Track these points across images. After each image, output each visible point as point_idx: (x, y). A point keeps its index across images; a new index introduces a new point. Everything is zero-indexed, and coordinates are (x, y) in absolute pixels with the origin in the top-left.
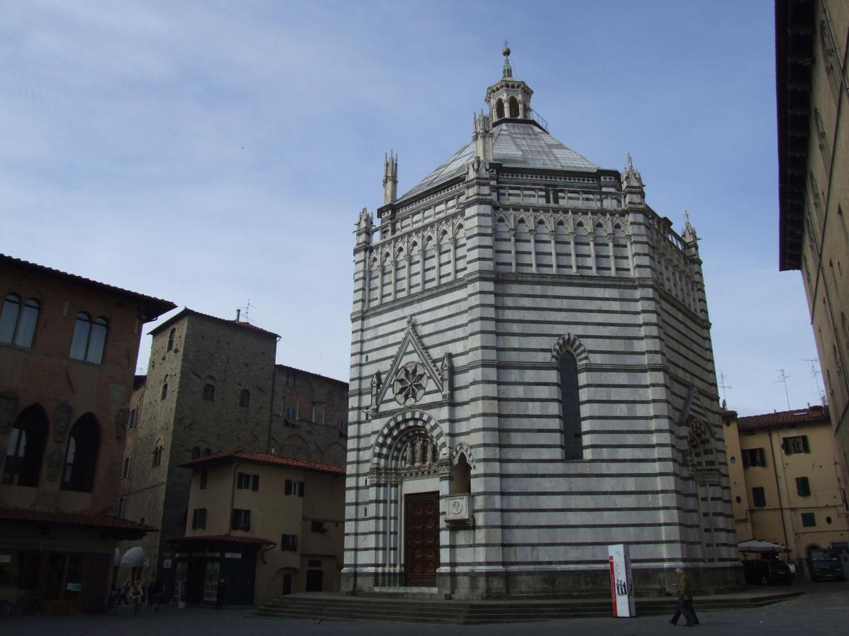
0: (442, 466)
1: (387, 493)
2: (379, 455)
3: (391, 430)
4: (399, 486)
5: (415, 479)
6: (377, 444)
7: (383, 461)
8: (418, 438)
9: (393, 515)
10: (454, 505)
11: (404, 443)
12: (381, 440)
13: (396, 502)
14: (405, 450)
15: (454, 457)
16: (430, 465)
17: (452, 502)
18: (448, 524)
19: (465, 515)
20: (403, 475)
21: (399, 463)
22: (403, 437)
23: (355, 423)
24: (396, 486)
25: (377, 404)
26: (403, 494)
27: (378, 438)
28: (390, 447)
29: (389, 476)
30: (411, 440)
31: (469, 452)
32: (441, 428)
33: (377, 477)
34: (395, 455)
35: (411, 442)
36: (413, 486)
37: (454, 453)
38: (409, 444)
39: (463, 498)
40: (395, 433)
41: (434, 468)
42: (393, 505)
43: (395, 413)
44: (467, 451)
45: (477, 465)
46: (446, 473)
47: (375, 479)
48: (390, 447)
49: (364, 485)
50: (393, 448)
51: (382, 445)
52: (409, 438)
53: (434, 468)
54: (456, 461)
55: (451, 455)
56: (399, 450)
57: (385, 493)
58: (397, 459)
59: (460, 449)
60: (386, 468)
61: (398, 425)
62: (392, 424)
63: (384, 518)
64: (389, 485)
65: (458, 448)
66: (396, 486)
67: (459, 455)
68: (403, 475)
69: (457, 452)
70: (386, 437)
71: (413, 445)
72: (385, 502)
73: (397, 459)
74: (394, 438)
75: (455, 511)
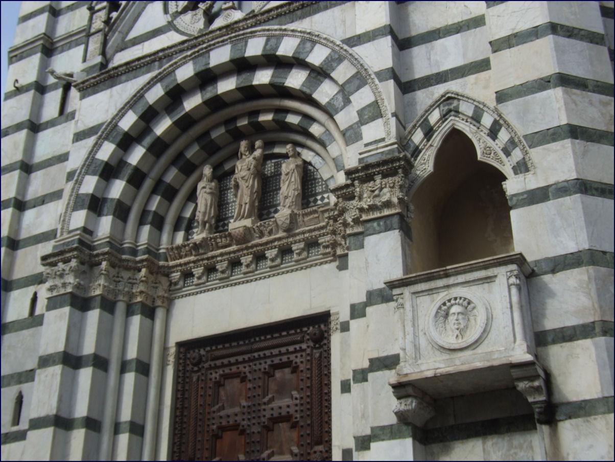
0: (370, 178)
1: (111, 332)
2: (96, 204)
3: (149, 116)
4: (160, 314)
5: (226, 282)
6: (90, 166)
7: (105, 225)
8: (243, 144)
9: (126, 415)
10: (443, 313)
11: (189, 169)
12: (107, 151)
13: (143, 368)
14: (192, 196)
15: (417, 151)
16: (293, 217)
17: (428, 305)
18: (410, 404)
19: (508, 346)
20: (176, 275)
21: (165, 238)
22: (188, 146)
23: (18, 127)
24: (149, 313)
25: (103, 53)
26: (172, 342)
27: (97, 146)
28: (136, 178)
29: (126, 275)
30: (216, 158)
31: (487, 120)
32: (355, 61)
33: (77, 273)
34: (154, 206)
35: (216, 168)
36: (207, 312)
37: (418, 137)
38: (207, 170)
39: (489, 279)
40: (162, 126)
41: (305, 227)
42: (130, 378)
43: (169, 57)
44: (476, 118)
45: (536, 154)
46: (388, 204)
47: (71, 279)
48: (136, 178)
49: (26, 313)
50: (148, 184)
51: (109, 172)
52: (210, 148)
53: (305, 227)
54: (425, 165)
55: (403, 142)
56: (170, 194)
57: (105, 333)
58: (158, 223)
59: (444, 117)
60: (114, 244)
61: (176, 94)
62: (156, 94)
63: (92, 424)
64: (121, 308)
65: (435, 117)
66: (149, 313)
67: (437, 140)
68: (176, 275)
69: (429, 133)
70: (126, 142)
71: (222, 176)
72: (100, 363)
73: (158, 223)
74: (158, 148)
75: (451, 340)
